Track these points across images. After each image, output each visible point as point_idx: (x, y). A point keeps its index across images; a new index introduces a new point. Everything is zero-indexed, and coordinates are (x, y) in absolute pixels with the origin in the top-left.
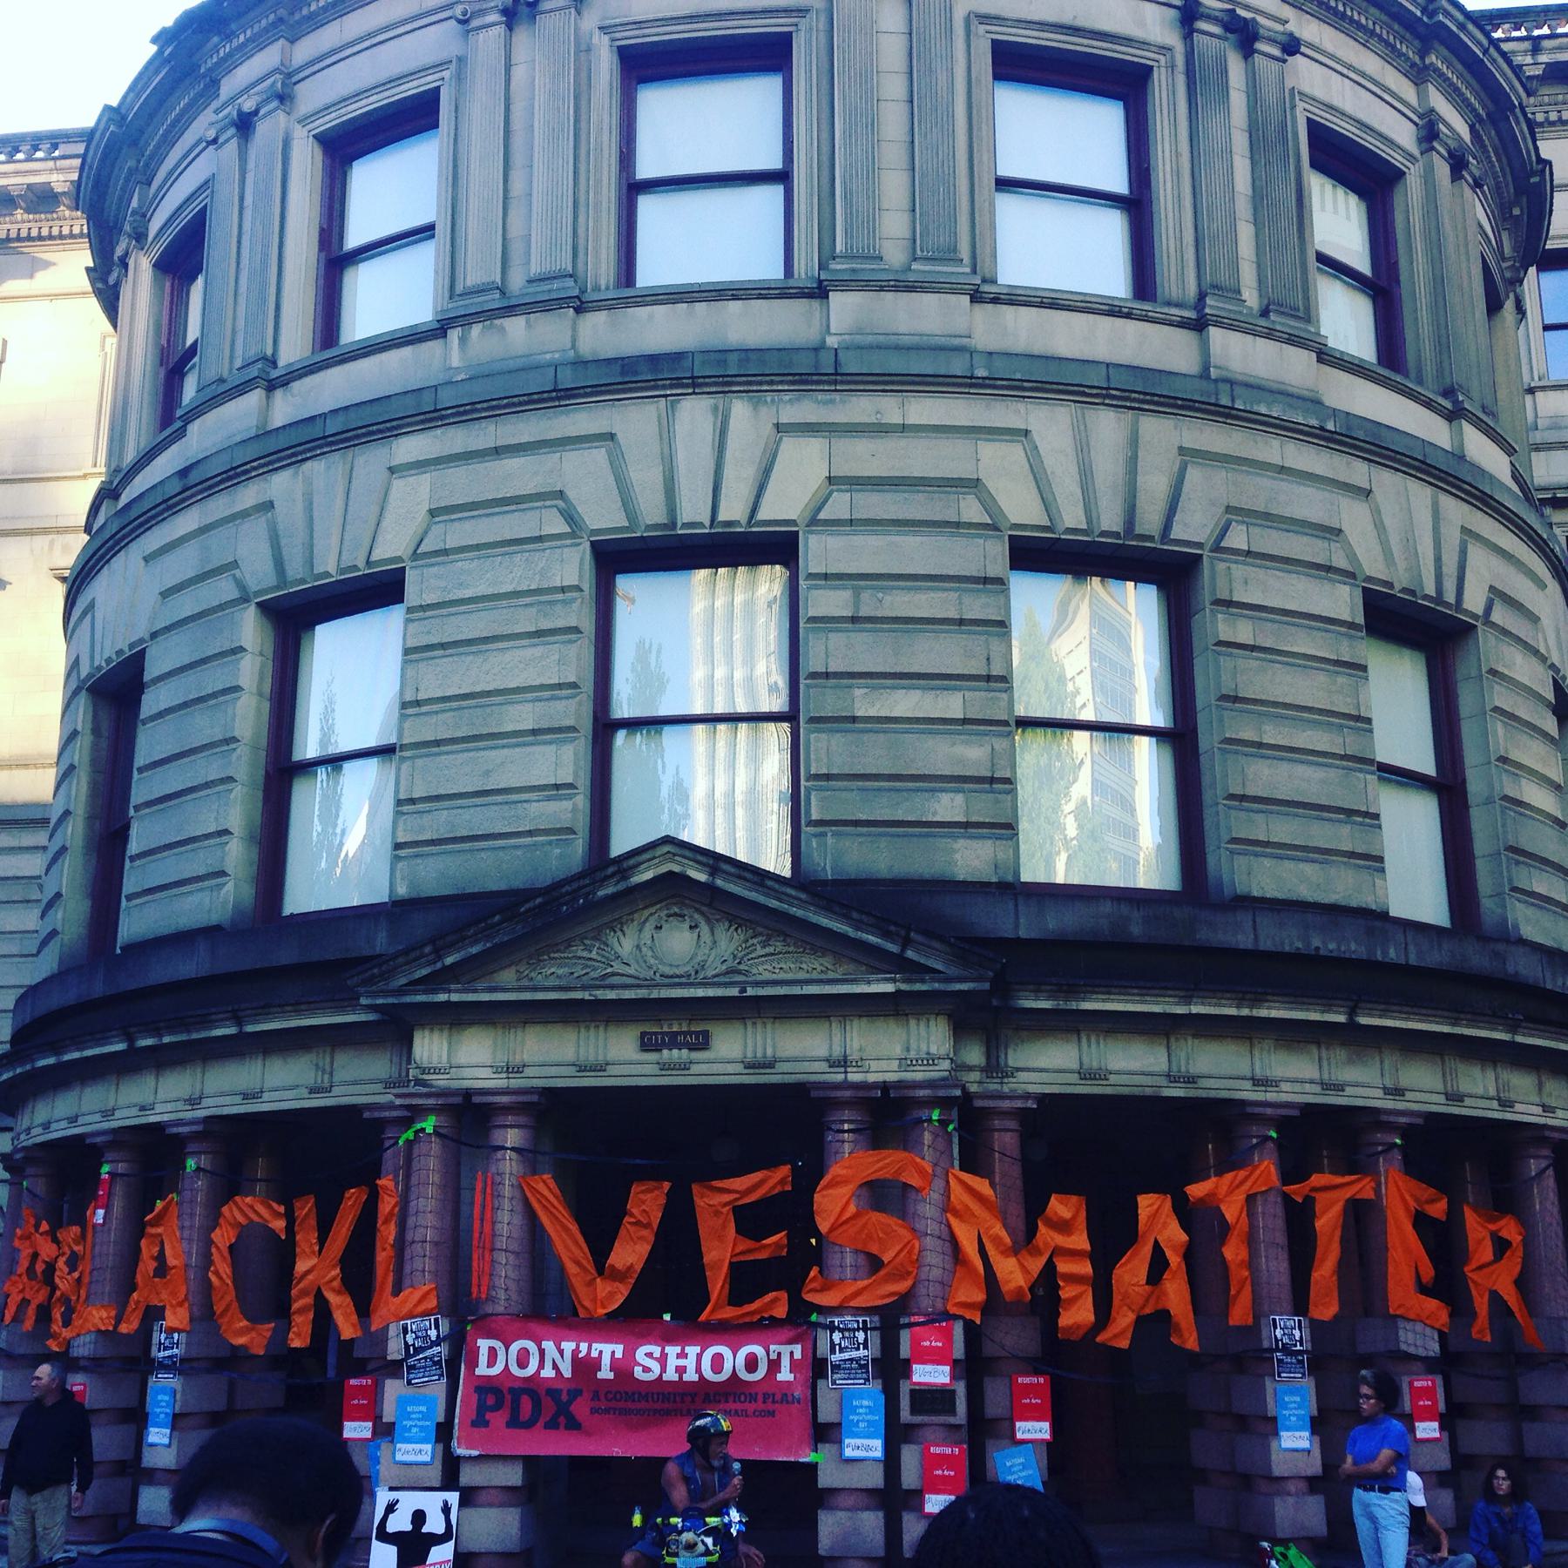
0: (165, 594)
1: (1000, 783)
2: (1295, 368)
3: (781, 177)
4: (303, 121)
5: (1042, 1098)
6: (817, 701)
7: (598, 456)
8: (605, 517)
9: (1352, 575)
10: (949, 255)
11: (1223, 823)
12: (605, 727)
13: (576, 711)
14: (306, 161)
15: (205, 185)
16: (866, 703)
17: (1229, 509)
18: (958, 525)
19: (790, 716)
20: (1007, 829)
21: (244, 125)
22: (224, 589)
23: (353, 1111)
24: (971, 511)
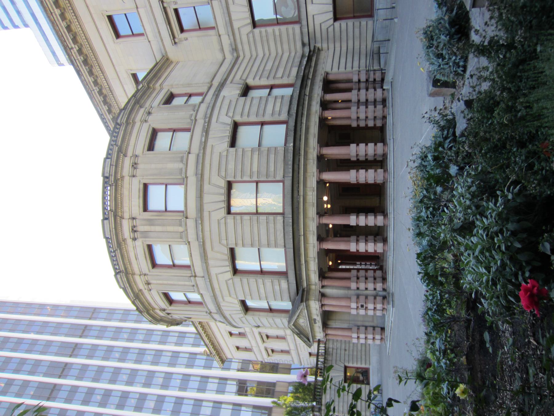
0: (230, 296)
1: (269, 150)
2: (203, 107)
3: (166, 185)
4: (149, 271)
5: (318, 143)
6: (255, 178)
7: (213, 214)
8: (223, 212)
9: (237, 99)
10: (182, 157)
11: (276, 118)
12: (257, 213)
13: (255, 217)
14: (156, 271)
15: (158, 292)
16: (255, 169)
17: (226, 115)
18: (227, 155)
19: (257, 183)
20: (276, 148)
21: (148, 284)
22: (230, 282)
23: (318, 253)
24: (225, 153)
